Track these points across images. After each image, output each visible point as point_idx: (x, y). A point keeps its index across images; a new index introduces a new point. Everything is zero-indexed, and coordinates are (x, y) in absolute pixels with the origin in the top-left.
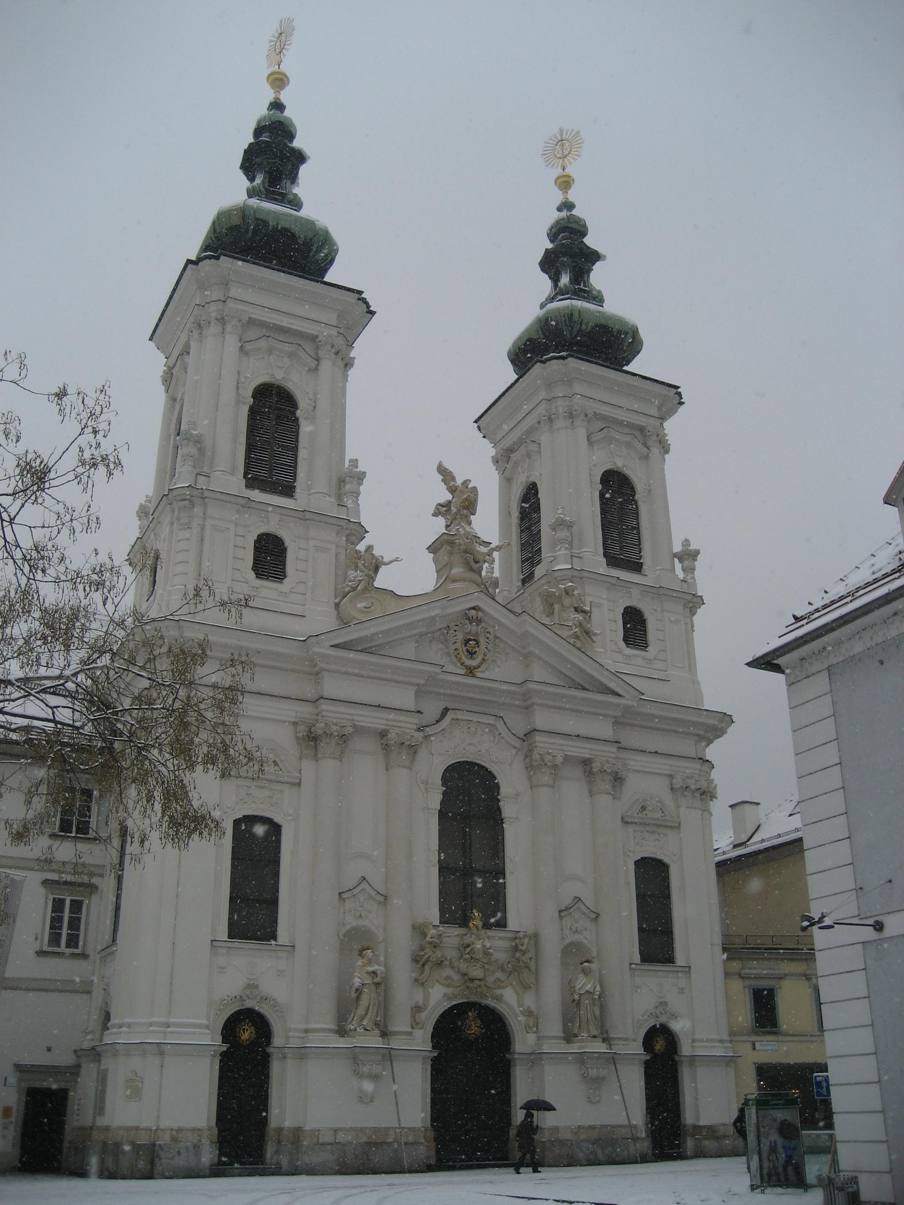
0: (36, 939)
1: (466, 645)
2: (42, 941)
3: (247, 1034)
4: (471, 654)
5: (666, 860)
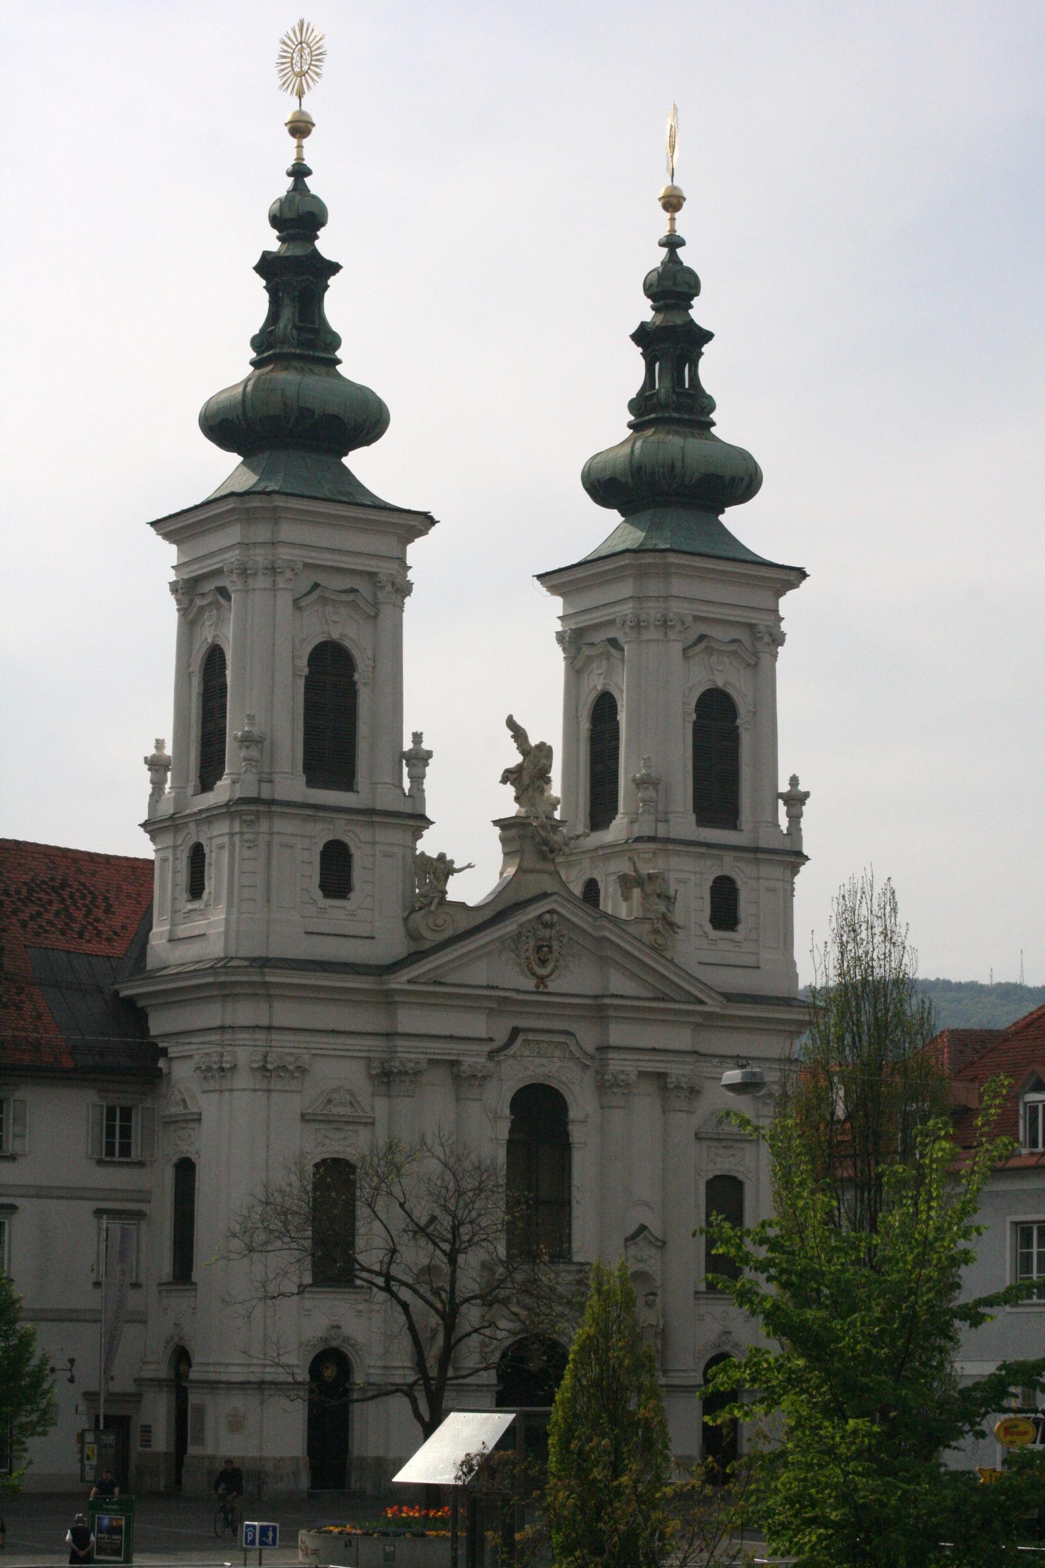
0: (93, 1270)
1: (538, 953)
2: (98, 1272)
3: (329, 1372)
4: (543, 962)
5: (741, 1177)
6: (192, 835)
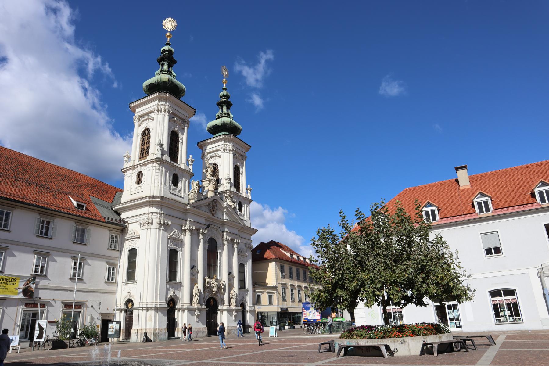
4: (214, 210)
6: (139, 169)
